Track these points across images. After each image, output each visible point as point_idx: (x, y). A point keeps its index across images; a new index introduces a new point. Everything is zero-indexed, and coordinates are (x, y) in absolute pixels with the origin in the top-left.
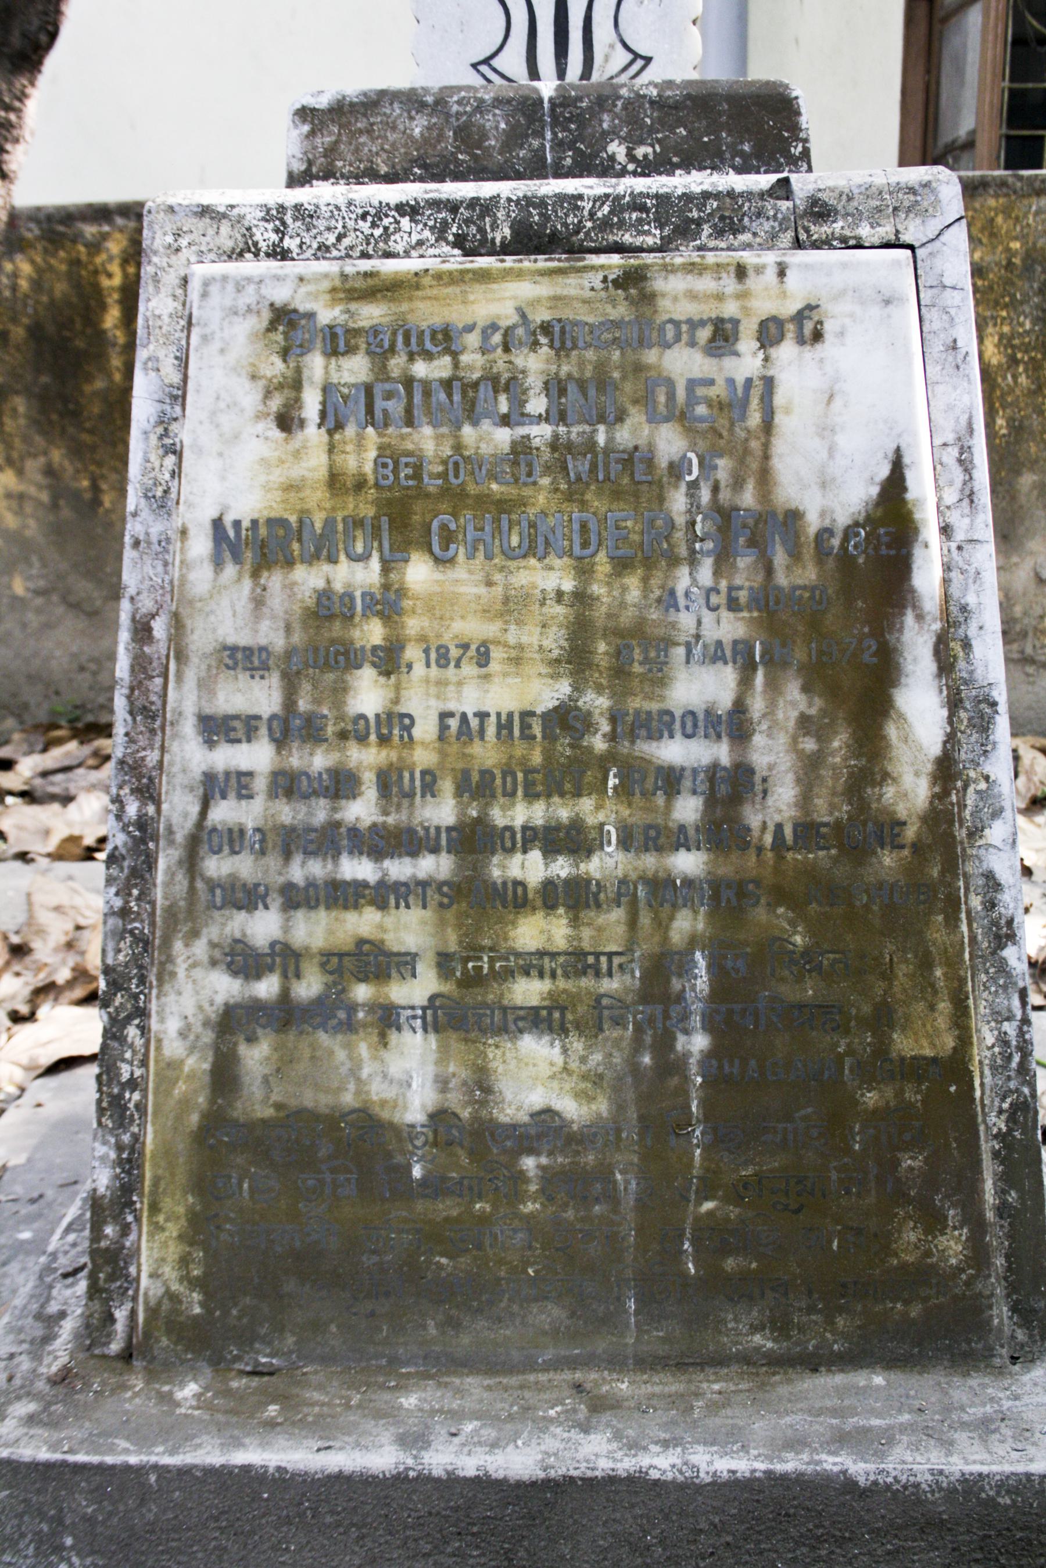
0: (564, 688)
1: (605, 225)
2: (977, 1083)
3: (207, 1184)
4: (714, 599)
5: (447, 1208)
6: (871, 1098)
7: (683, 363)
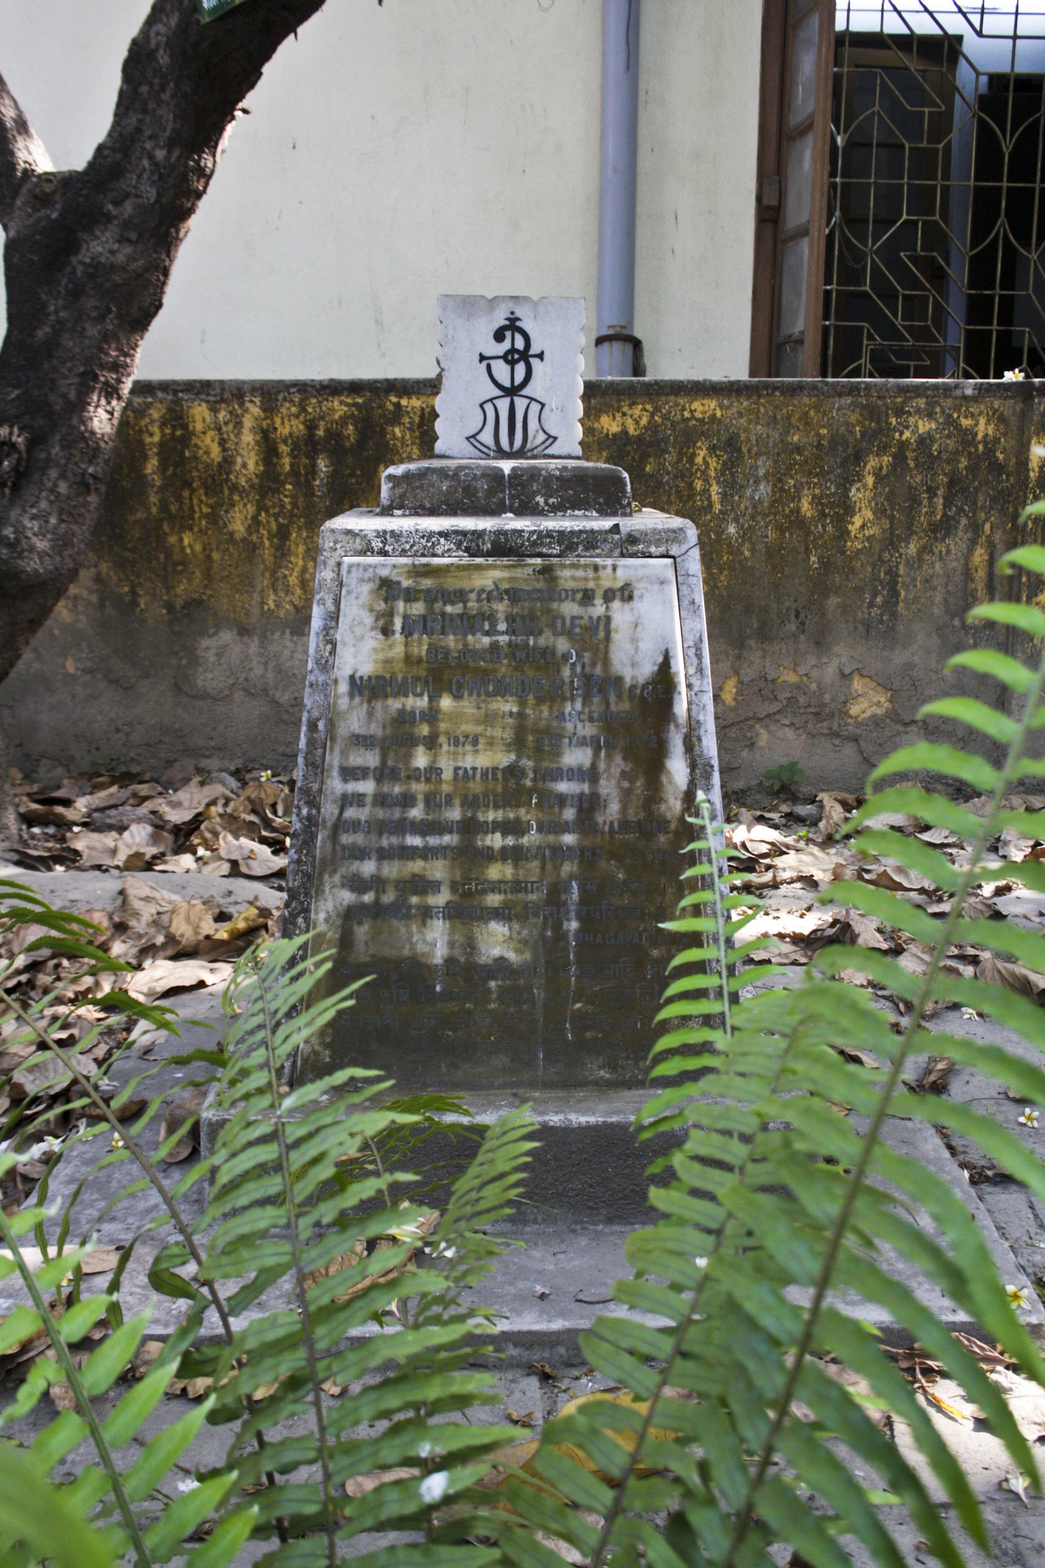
0: (513, 757)
1: (534, 544)
4: (582, 717)
5: (453, 1006)
7: (569, 609)
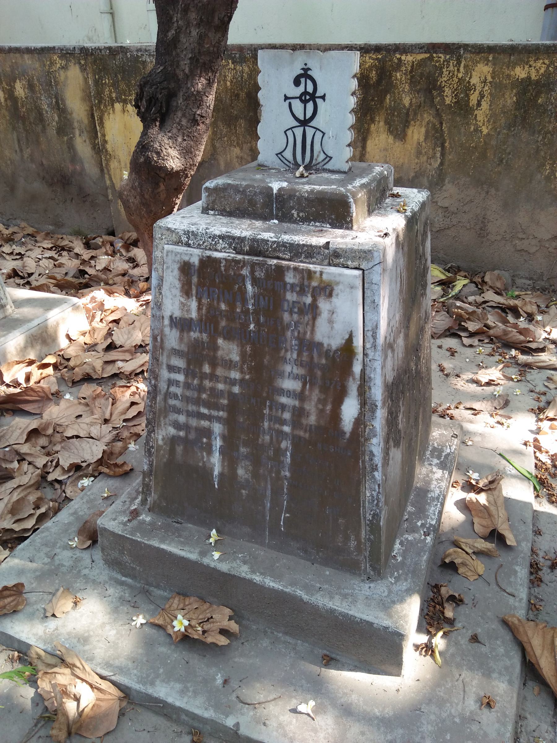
1: (275, 250)
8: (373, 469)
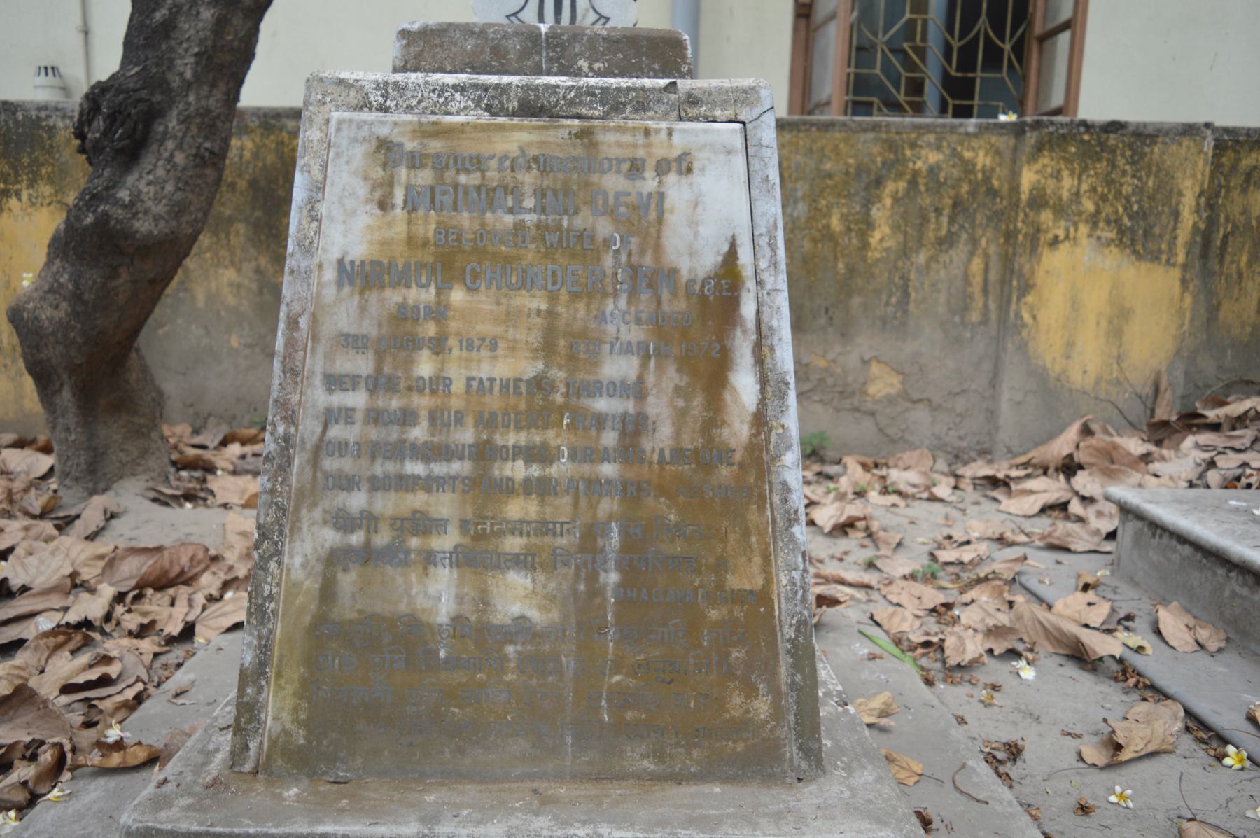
0: (540, 366)
1: (572, 103)
2: (776, 607)
3: (313, 661)
4: (627, 318)
5: (459, 677)
6: (714, 614)
7: (613, 182)
8: (789, 520)
